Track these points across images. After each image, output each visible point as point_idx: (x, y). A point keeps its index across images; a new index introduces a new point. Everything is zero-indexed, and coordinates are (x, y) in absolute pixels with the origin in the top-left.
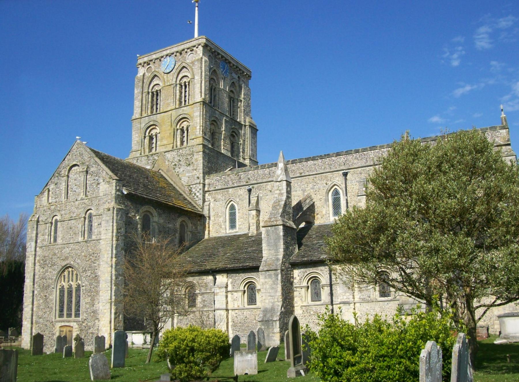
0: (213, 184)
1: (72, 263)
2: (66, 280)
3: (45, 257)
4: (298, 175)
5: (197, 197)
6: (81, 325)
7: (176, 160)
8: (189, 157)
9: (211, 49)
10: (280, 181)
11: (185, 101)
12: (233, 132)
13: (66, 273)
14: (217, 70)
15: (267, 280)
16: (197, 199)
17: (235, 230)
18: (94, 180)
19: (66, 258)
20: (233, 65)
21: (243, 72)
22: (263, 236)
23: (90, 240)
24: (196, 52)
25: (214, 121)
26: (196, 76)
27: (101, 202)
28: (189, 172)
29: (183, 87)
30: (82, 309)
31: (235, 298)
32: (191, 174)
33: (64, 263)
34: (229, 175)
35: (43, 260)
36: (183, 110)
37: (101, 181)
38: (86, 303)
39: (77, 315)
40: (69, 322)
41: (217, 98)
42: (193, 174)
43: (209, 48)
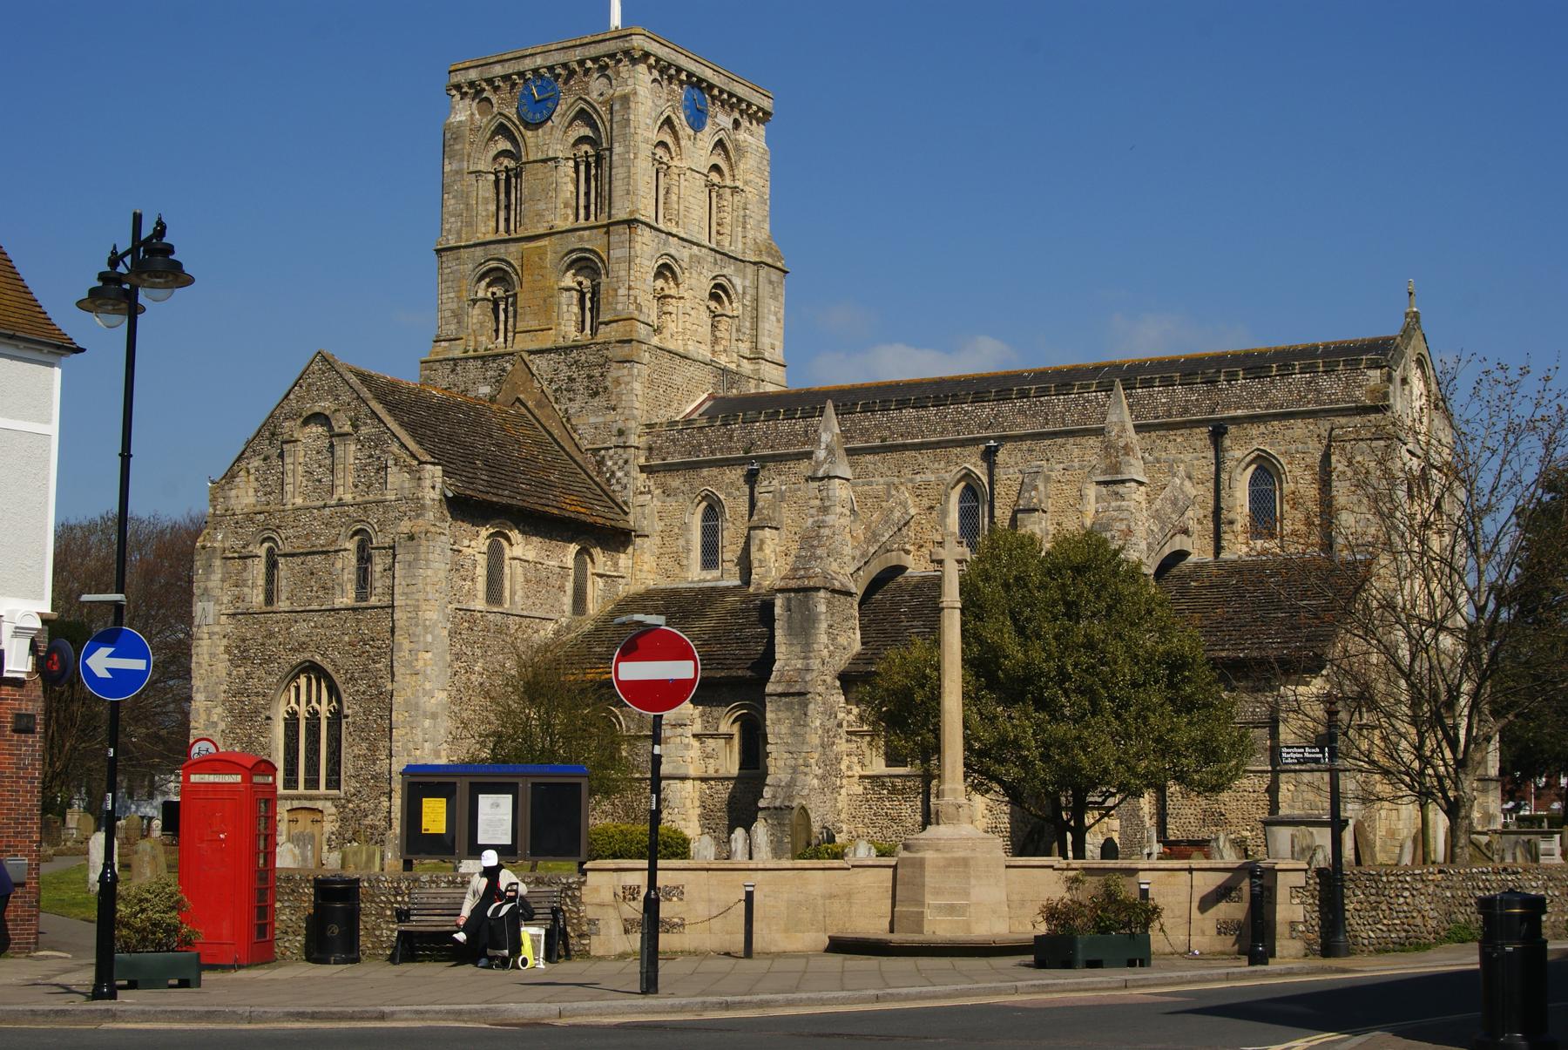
0: (660, 448)
1: (318, 658)
2: (303, 698)
3: (244, 640)
4: (878, 443)
5: (618, 482)
6: (344, 807)
7: (562, 376)
8: (597, 373)
9: (658, 60)
10: (822, 479)
11: (587, 208)
12: (717, 286)
13: (303, 681)
14: (674, 117)
15: (781, 715)
16: (617, 488)
17: (716, 573)
18: (371, 456)
19: (303, 646)
20: (721, 91)
21: (749, 105)
22: (777, 610)
23: (364, 604)
24: (618, 73)
25: (665, 266)
26: (616, 145)
27: (392, 515)
28: (595, 412)
29: (582, 168)
30: (347, 767)
31: (709, 750)
32: (601, 419)
33: (299, 658)
34: (701, 428)
35: (238, 647)
36: (581, 239)
37: (390, 463)
38: (357, 757)
39: (334, 783)
40: (311, 798)
41: (674, 198)
42: (609, 418)
43: (652, 60)
